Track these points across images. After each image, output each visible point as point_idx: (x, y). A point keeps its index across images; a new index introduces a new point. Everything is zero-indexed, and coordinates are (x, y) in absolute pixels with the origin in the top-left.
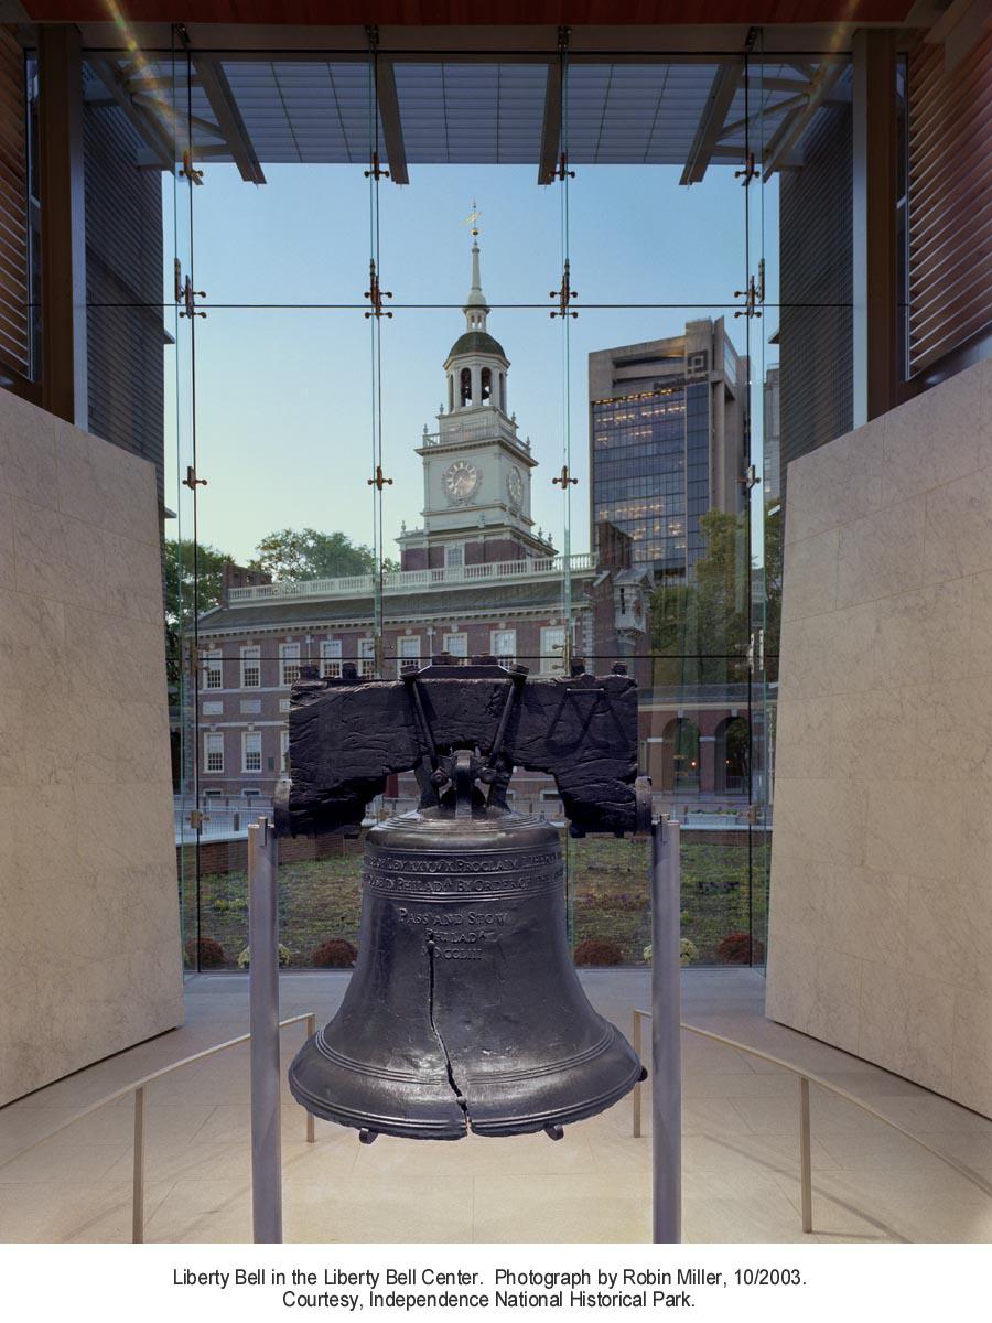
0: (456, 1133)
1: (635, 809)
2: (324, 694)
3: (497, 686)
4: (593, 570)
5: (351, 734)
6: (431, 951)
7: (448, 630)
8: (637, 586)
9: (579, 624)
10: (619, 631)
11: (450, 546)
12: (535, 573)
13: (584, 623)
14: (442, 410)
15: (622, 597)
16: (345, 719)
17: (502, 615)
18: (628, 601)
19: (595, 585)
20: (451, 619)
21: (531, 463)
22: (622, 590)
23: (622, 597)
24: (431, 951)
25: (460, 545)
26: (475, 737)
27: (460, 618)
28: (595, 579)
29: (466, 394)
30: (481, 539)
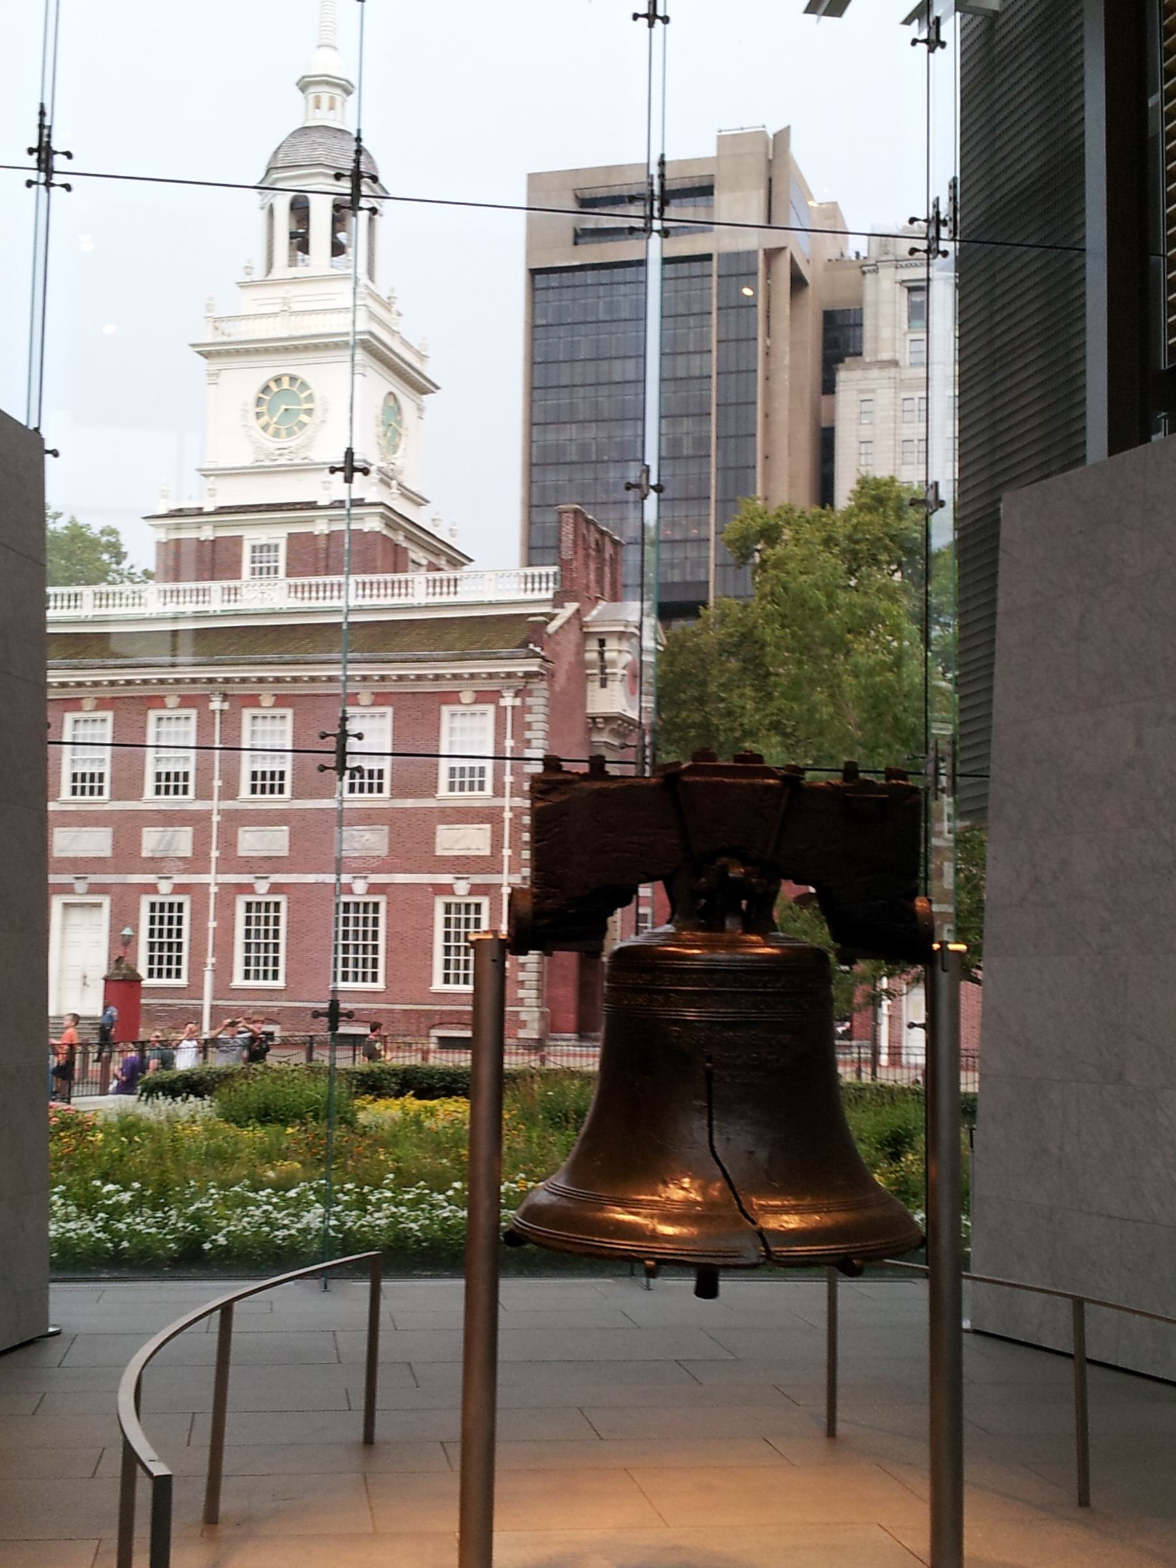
4: (547, 600)
7: (253, 701)
9: (518, 702)
10: (593, 719)
11: (253, 536)
13: (529, 701)
14: (248, 269)
15: (601, 654)
17: (365, 678)
18: (613, 663)
19: (552, 627)
20: (261, 680)
21: (421, 386)
22: (602, 643)
23: (601, 654)
25: (277, 535)
27: (278, 680)
28: (552, 617)
29: (301, 242)
30: (321, 527)
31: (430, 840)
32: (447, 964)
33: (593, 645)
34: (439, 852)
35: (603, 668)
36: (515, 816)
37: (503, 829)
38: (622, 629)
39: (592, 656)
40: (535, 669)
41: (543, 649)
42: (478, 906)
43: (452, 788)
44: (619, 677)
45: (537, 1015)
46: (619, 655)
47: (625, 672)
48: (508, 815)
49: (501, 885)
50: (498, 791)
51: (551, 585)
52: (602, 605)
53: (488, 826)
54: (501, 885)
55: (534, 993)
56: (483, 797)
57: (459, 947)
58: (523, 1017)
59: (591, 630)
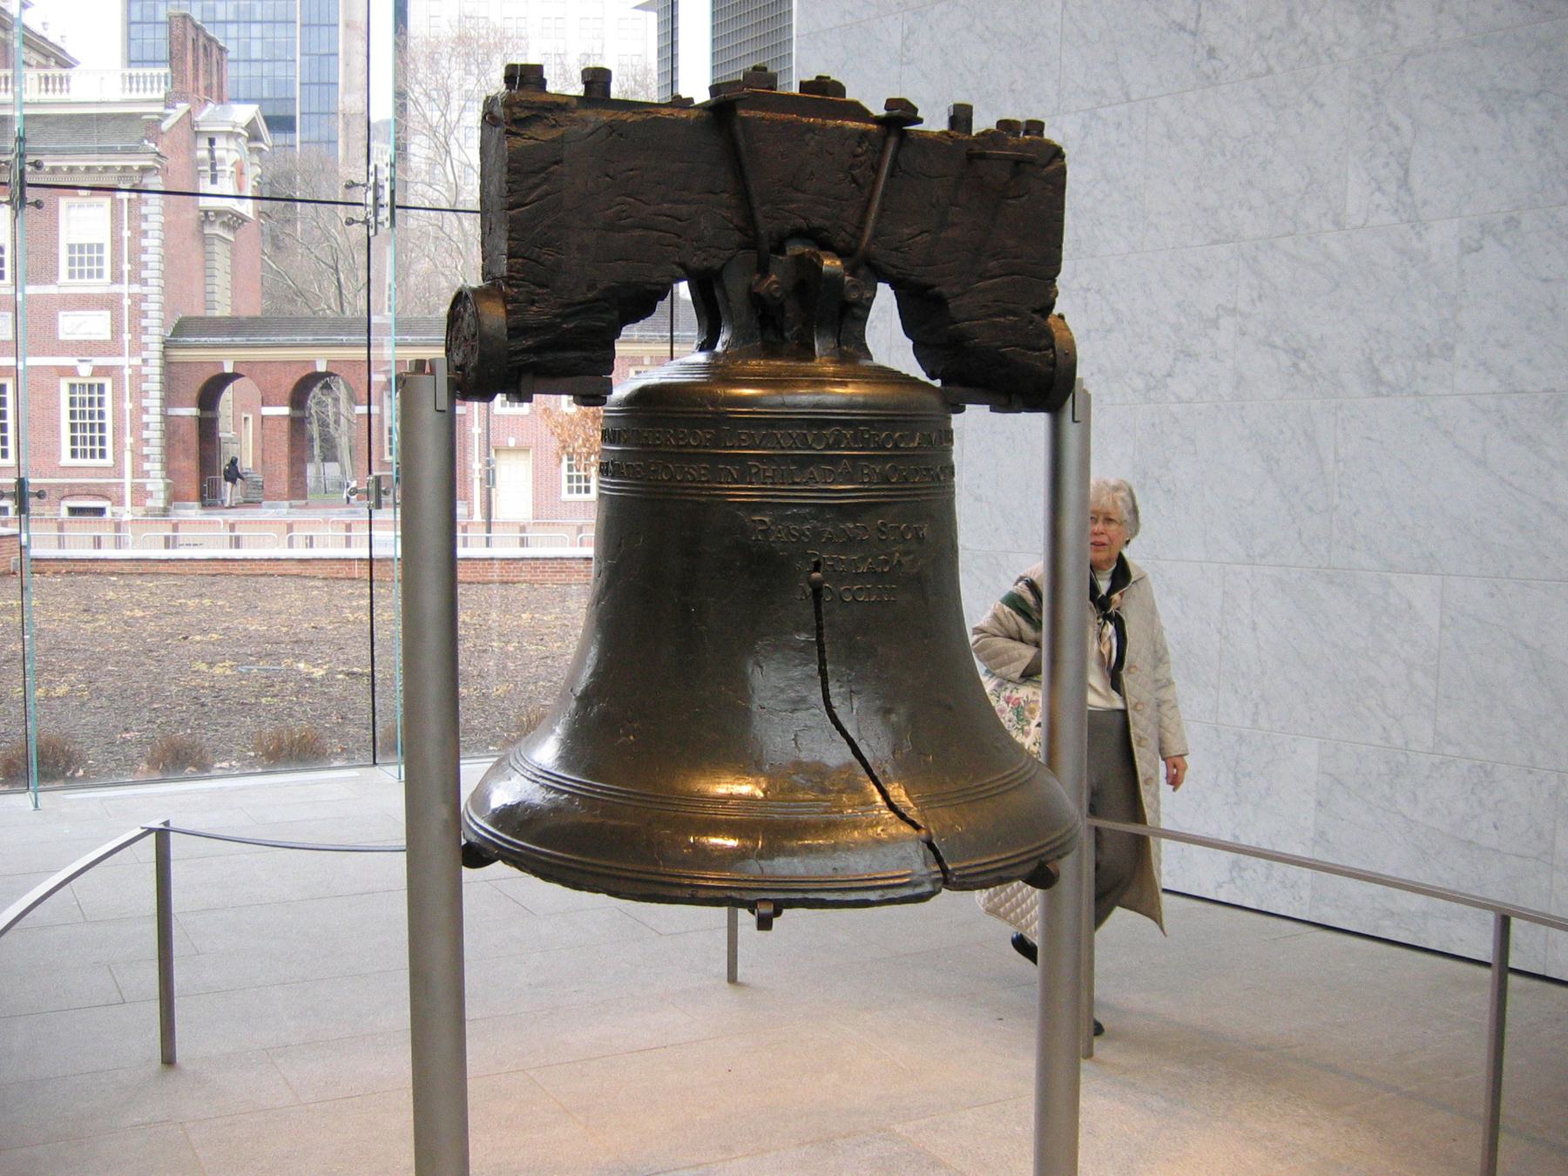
0: (928, 888)
1: (1054, 364)
2: (573, 121)
3: (864, 135)
4: (158, 101)
5: (618, 199)
6: (817, 591)
8: (239, 135)
10: (206, 212)
12: (44, 97)
15: (211, 151)
16: (611, 174)
18: (223, 161)
19: (165, 126)
22: (212, 142)
23: (211, 151)
24: (817, 591)
26: (828, 224)
31: (52, 326)
32: (73, 441)
33: (204, 143)
34: (62, 337)
35: (213, 166)
36: (134, 303)
37: (122, 315)
38: (230, 129)
39: (203, 154)
40: (150, 163)
41: (156, 145)
42: (101, 388)
43: (71, 275)
44: (228, 173)
45: (162, 486)
46: (228, 152)
47: (233, 169)
48: (127, 302)
49: (122, 367)
50: (117, 278)
51: (163, 85)
52: (211, 105)
53: (107, 313)
54: (122, 367)
55: (158, 466)
56: (100, 286)
57: (85, 424)
58: (149, 488)
59: (202, 129)
